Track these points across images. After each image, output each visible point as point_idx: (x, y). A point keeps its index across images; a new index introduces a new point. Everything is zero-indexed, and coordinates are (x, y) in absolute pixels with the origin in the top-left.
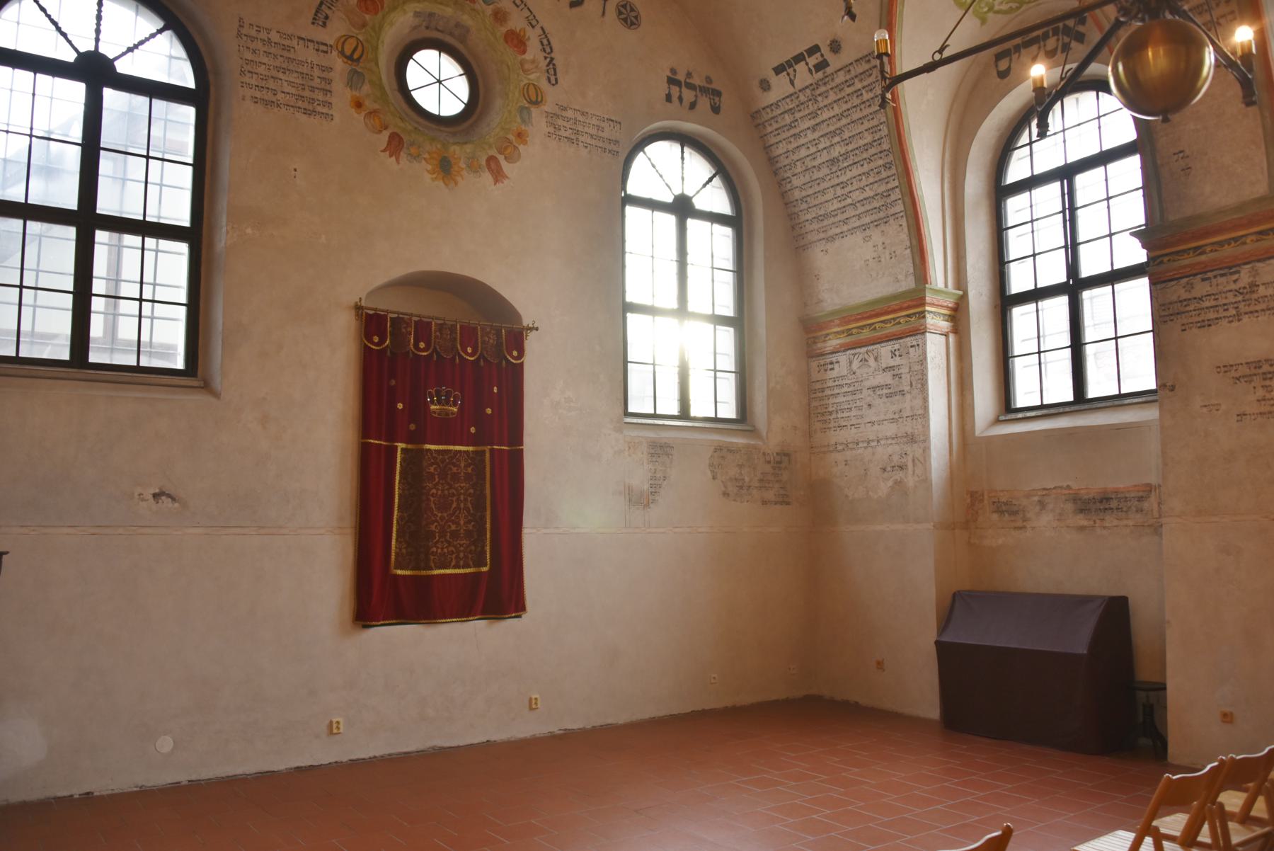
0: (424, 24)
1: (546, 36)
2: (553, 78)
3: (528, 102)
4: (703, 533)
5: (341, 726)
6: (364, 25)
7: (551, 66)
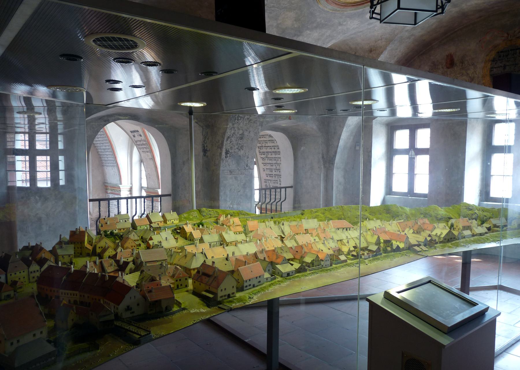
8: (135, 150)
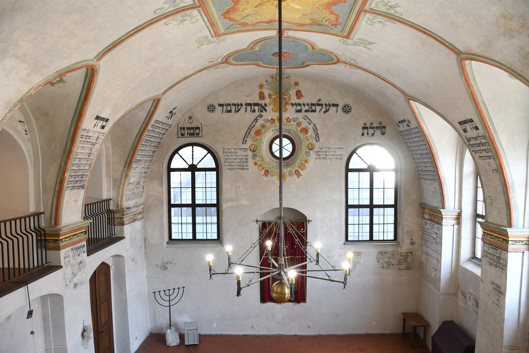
0: (277, 132)
1: (315, 126)
2: (318, 140)
3: (309, 150)
4: (372, 280)
5: (255, 326)
6: (256, 140)
7: (317, 135)
8: (468, 155)
